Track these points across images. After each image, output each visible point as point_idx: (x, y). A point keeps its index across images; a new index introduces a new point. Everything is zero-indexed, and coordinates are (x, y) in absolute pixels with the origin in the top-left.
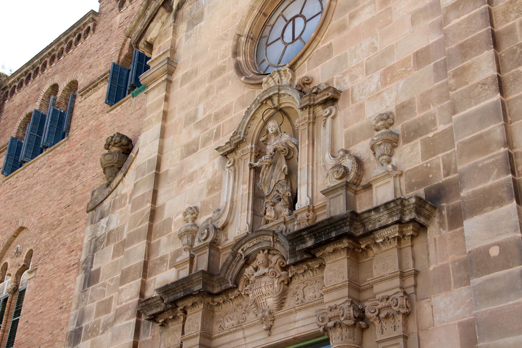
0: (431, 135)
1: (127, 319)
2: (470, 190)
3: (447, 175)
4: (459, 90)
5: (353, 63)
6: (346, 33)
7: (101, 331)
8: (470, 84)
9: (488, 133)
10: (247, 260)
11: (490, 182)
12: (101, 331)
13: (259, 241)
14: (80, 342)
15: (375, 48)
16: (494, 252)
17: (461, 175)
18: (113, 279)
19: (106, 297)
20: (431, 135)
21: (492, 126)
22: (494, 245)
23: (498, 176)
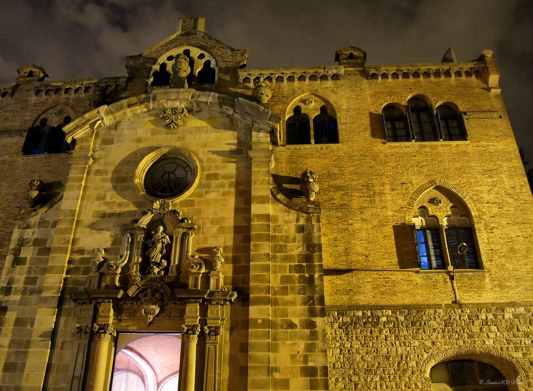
0: (238, 265)
1: (52, 294)
2: (254, 295)
3: (244, 284)
4: (254, 253)
5: (204, 216)
6: (201, 199)
7: (28, 294)
8: (260, 252)
9: (264, 275)
10: (181, 313)
11: (262, 295)
12: (28, 294)
13: (152, 284)
14: (10, 295)
15: (217, 214)
16: (260, 321)
17: (299, 317)
18: (37, 267)
19: (32, 276)
20: (238, 265)
21: (265, 273)
22: (260, 319)
23: (265, 294)
